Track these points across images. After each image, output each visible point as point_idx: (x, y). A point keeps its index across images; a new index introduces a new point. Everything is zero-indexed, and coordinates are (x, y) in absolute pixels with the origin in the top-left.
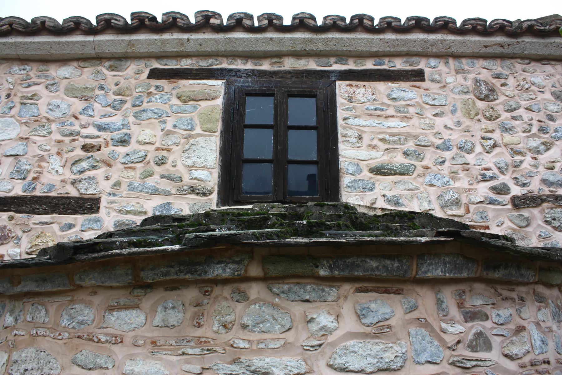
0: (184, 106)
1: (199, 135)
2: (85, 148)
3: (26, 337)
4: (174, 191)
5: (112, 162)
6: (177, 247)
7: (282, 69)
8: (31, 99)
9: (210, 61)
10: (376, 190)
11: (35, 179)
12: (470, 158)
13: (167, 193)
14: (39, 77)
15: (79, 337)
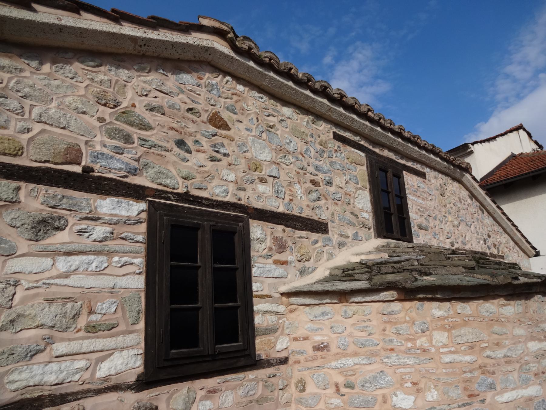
1: (360, 189)
2: (312, 181)
4: (357, 225)
5: (328, 197)
6: (539, 280)
7: (382, 154)
8: (272, 128)
9: (358, 137)
10: (421, 237)
11: (291, 200)
12: (442, 226)
14: (274, 110)
15: (492, 320)
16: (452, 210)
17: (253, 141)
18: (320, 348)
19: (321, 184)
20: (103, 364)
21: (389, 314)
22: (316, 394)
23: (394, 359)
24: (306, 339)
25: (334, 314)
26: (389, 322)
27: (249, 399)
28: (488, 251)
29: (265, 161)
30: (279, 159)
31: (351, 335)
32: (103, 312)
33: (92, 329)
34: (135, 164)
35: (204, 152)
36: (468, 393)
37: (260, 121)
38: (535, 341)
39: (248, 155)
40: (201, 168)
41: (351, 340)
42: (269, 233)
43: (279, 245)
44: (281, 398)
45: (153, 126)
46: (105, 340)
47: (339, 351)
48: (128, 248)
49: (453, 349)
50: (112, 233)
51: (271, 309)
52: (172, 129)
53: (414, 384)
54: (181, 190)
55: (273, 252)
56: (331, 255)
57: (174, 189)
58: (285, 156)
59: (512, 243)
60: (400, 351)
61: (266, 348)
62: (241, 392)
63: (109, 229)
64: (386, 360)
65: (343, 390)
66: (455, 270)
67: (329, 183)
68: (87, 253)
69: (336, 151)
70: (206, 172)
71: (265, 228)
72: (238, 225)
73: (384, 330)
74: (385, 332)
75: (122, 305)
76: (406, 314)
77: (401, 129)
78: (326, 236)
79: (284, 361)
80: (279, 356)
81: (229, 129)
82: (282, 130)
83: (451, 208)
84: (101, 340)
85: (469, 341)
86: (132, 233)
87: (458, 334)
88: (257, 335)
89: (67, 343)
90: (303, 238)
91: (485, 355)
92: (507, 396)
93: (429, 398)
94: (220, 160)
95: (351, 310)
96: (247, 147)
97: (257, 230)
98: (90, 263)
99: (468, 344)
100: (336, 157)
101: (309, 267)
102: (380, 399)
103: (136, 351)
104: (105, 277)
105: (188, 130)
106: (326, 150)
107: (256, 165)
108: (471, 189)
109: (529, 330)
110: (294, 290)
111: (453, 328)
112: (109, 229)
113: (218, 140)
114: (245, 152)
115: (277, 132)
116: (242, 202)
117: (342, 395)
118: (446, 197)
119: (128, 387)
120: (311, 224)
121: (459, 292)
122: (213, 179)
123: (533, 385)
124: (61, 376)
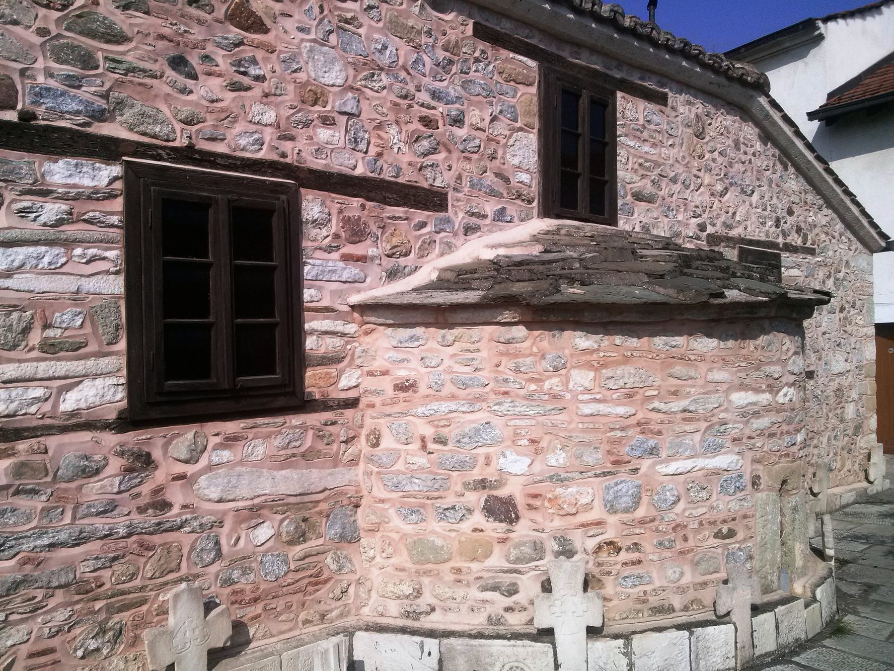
0: (505, 87)
1: (520, 129)
3: (620, 358)
4: (505, 195)
5: (451, 147)
8: (349, 24)
10: (636, 215)
11: (380, 155)
12: (687, 194)
13: (501, 196)
15: (673, 357)
16: (713, 165)
17: (311, 50)
18: (405, 387)
19: (440, 124)
20: (69, 394)
21: (508, 342)
22: (394, 450)
23: (506, 406)
24: (385, 373)
25: (427, 339)
26: (506, 354)
27: (290, 452)
28: (780, 240)
29: (333, 86)
30: (361, 80)
31: (449, 371)
32: (64, 326)
33: (50, 349)
34: (102, 103)
35: (220, 75)
36: (613, 458)
37: (326, 12)
38: (747, 391)
39: (302, 76)
40: (215, 104)
41: (448, 377)
42: (334, 212)
43: (353, 229)
44: (343, 454)
45: (130, 35)
46: (69, 363)
47: (430, 392)
48: (96, 236)
49: (598, 396)
50: (71, 214)
51: (333, 329)
52: (162, 37)
53: (533, 441)
54: (180, 142)
55: (342, 241)
56: (449, 247)
57: (167, 141)
58: (373, 75)
59: (839, 226)
60: (518, 396)
61: (322, 383)
62: (277, 442)
63: (64, 207)
64: (496, 408)
65: (431, 446)
66: (632, 277)
67: (458, 121)
68: (36, 243)
69: (477, 60)
70: (222, 110)
71: (328, 202)
72: (278, 199)
73: (498, 366)
74: (500, 369)
75: (91, 316)
76: (533, 344)
77: (616, 12)
78: (442, 215)
79: (353, 403)
80: (343, 395)
81: (266, 31)
82: (370, 26)
83: (714, 160)
84: (63, 363)
85: (627, 386)
86: (101, 212)
87: (611, 375)
88: (309, 366)
89: (17, 365)
90: (399, 218)
91: (651, 407)
92: (673, 467)
93: (553, 462)
94: (248, 89)
95: (451, 334)
96: (298, 62)
97: (312, 204)
98: (40, 258)
99: (625, 390)
100: (475, 71)
101: (406, 266)
102: (481, 460)
103: (115, 379)
104: (64, 277)
105: (190, 37)
106: (456, 58)
107: (316, 94)
108: (766, 123)
109: (739, 374)
110: (369, 302)
111: (605, 366)
112: (64, 207)
113: (247, 52)
114: (295, 71)
115: (361, 31)
116: (288, 160)
117: (430, 453)
118: (707, 138)
119: (106, 426)
120: (414, 196)
121: (621, 313)
122: (235, 120)
123: (725, 453)
124: (13, 407)
